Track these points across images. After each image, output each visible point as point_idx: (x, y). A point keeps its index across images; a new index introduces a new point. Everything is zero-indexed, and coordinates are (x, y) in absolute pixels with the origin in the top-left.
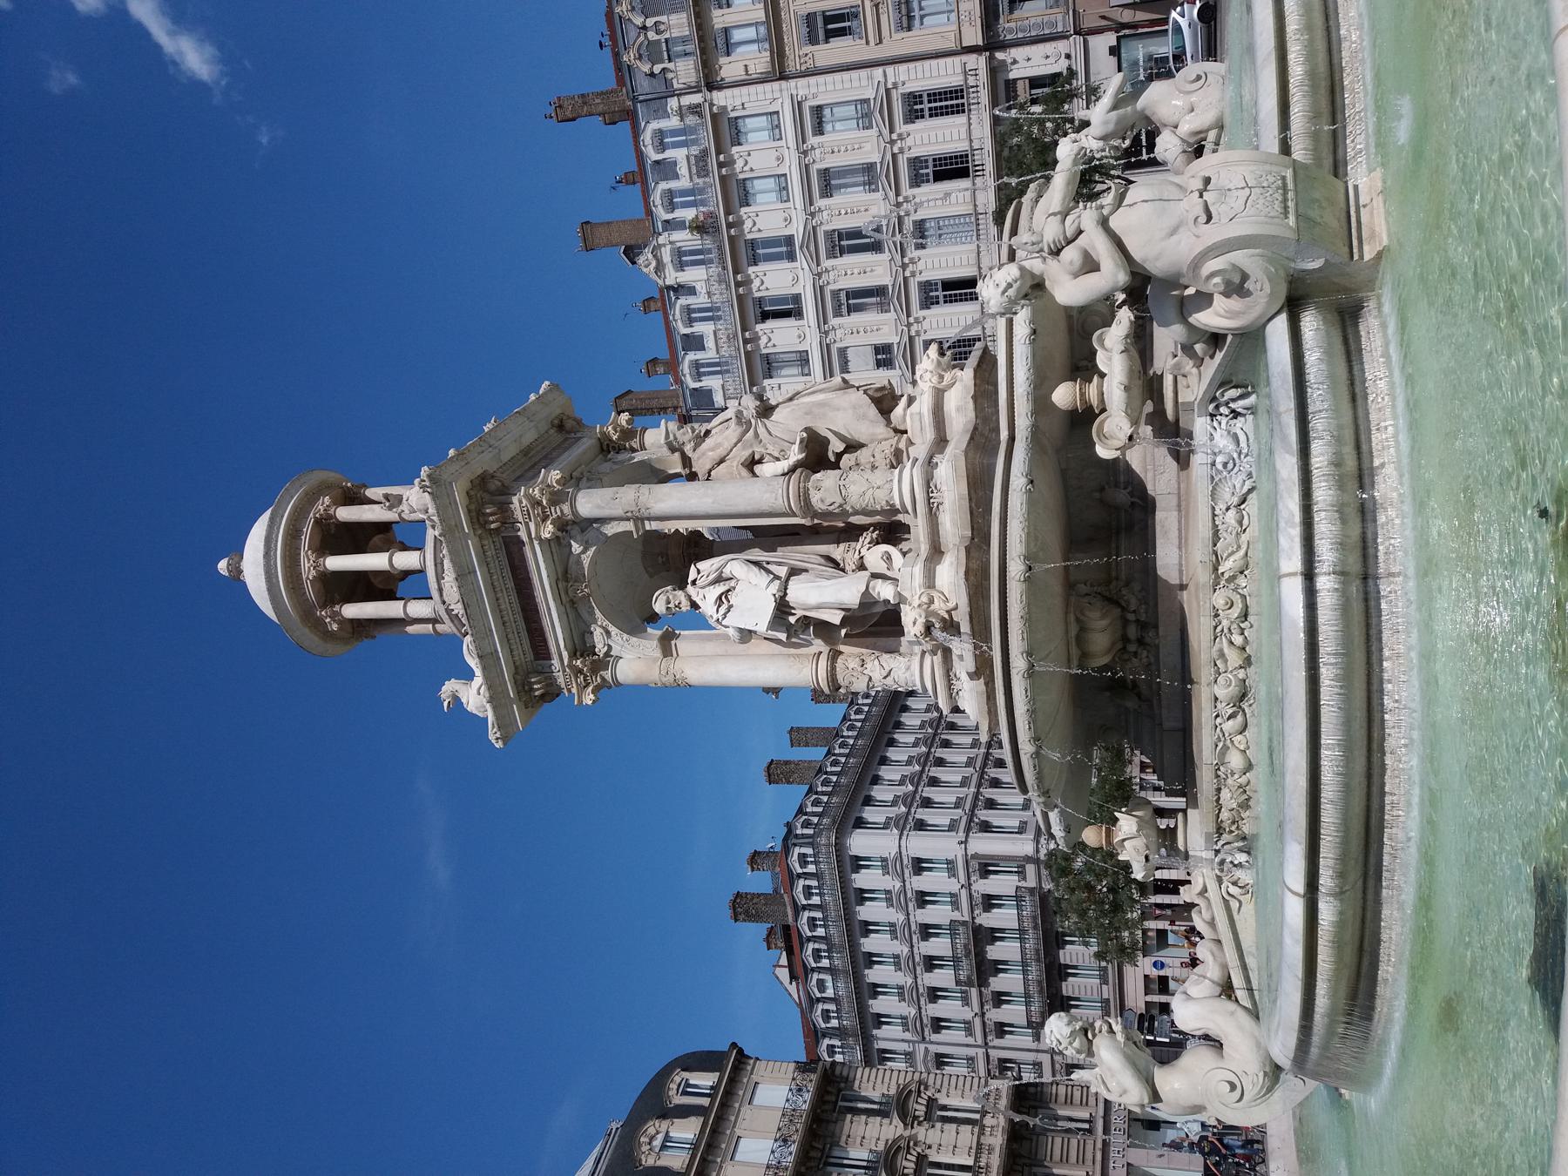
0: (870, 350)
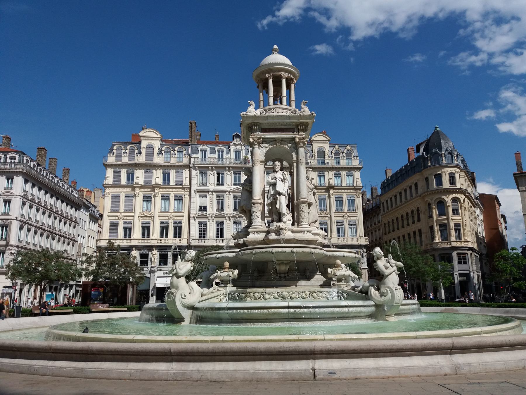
0: (205, 205)
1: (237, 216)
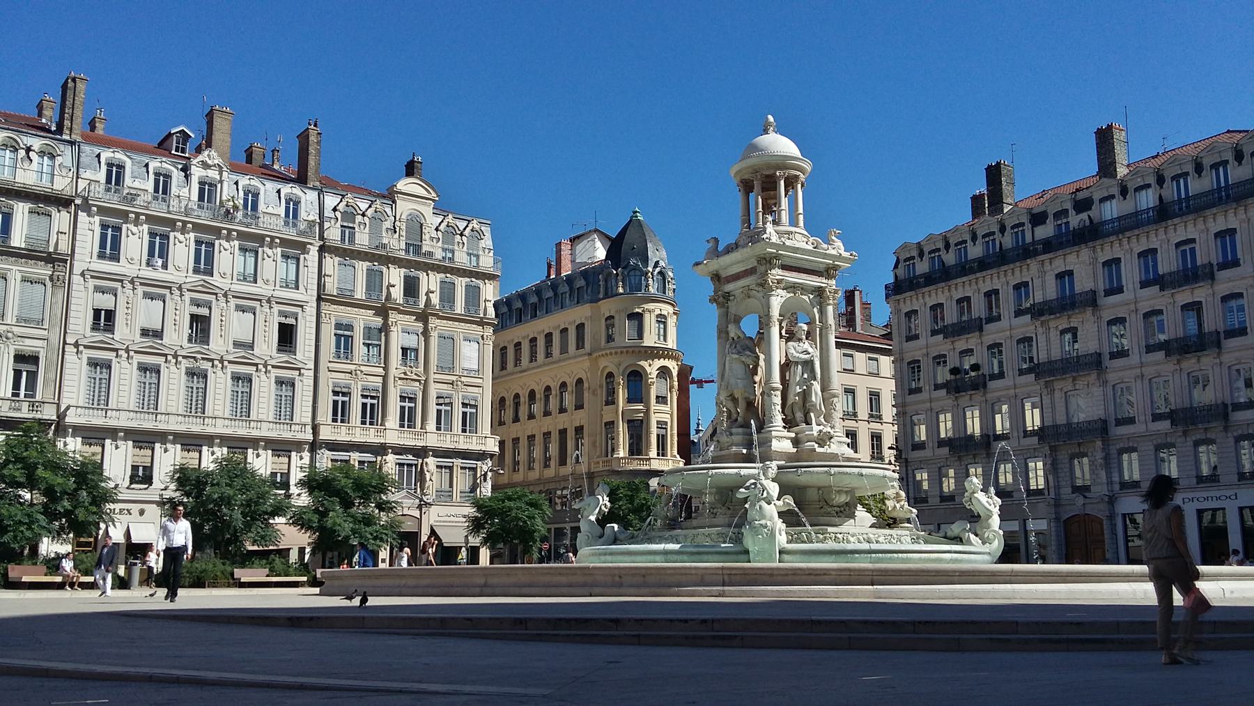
1: (199, 356)
